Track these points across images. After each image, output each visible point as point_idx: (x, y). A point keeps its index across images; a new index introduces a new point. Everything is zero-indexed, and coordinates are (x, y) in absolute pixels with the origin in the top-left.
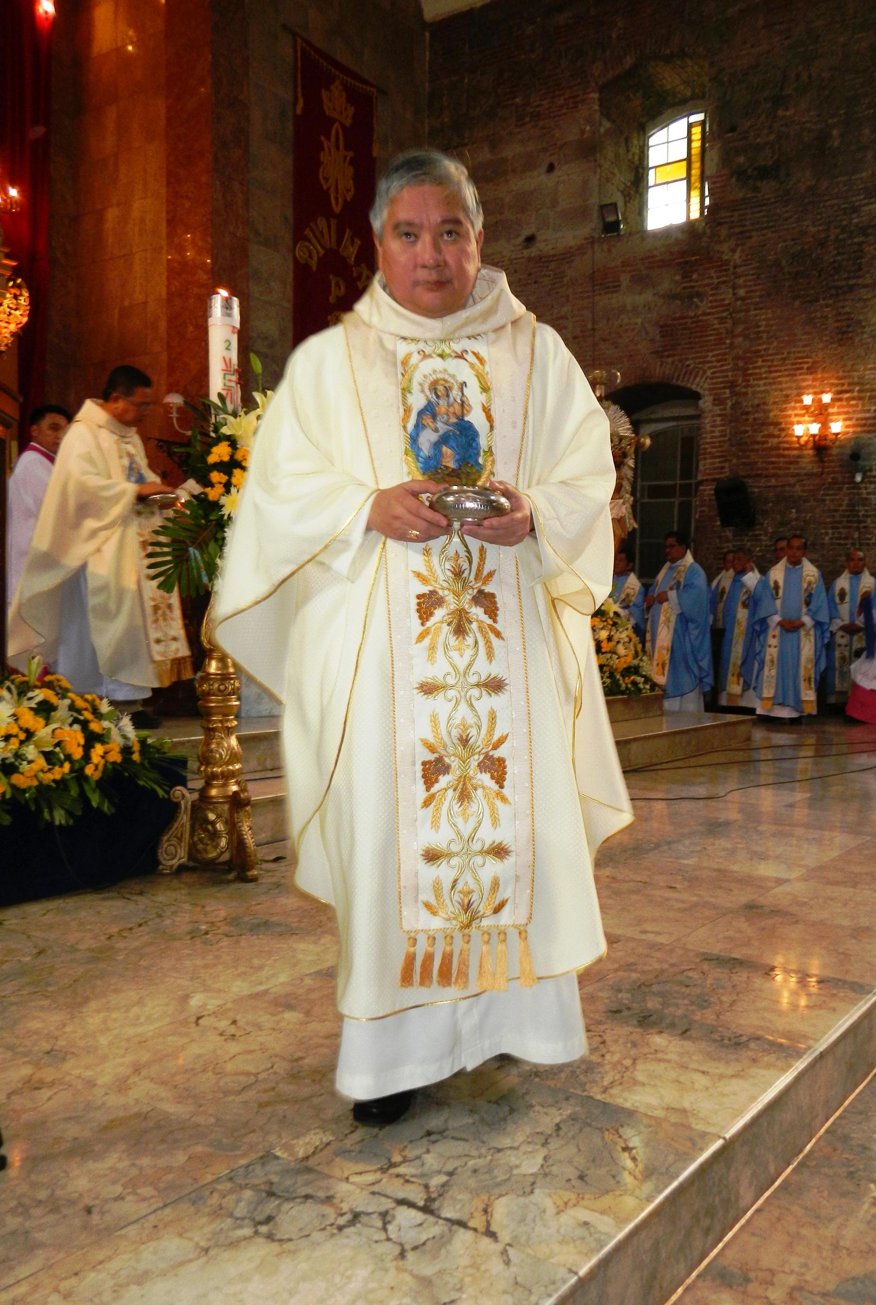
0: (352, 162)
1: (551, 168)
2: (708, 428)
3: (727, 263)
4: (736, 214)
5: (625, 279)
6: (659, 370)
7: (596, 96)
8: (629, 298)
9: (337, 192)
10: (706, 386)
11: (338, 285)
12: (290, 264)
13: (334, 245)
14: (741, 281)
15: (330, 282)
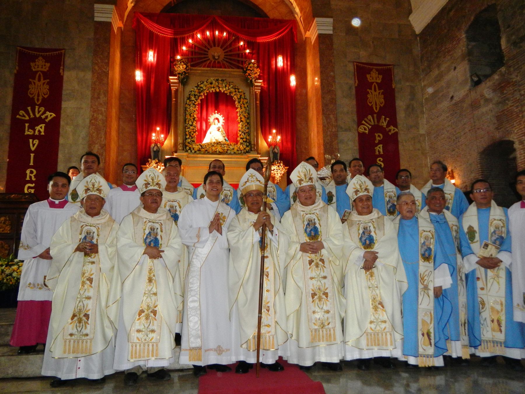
0: (383, 93)
1: (455, 68)
2: (518, 156)
3: (516, 82)
4: (515, 60)
5: (482, 102)
6: (498, 135)
7: (464, 36)
8: (484, 110)
9: (376, 105)
10: (515, 137)
11: (379, 136)
12: (357, 134)
13: (376, 123)
14: (521, 88)
15: (375, 136)
